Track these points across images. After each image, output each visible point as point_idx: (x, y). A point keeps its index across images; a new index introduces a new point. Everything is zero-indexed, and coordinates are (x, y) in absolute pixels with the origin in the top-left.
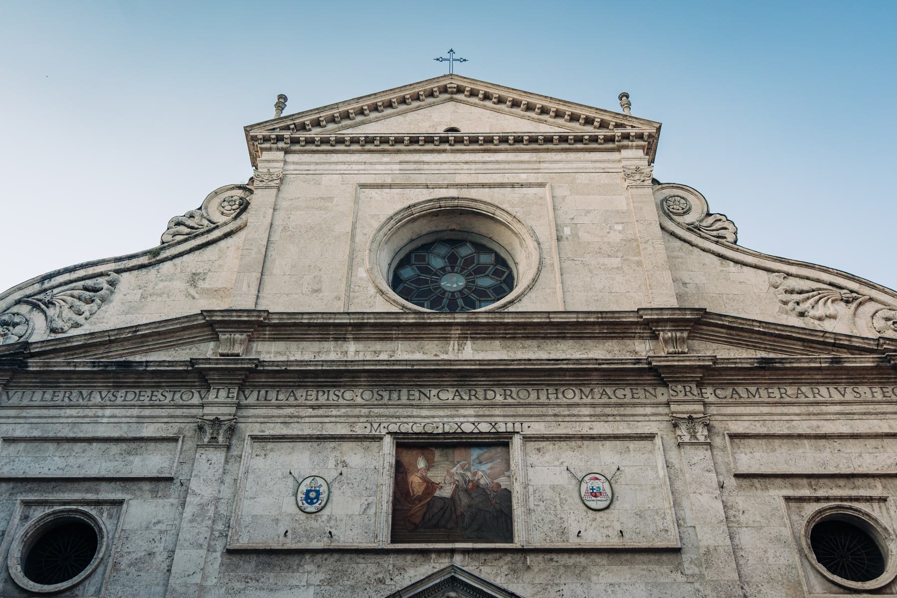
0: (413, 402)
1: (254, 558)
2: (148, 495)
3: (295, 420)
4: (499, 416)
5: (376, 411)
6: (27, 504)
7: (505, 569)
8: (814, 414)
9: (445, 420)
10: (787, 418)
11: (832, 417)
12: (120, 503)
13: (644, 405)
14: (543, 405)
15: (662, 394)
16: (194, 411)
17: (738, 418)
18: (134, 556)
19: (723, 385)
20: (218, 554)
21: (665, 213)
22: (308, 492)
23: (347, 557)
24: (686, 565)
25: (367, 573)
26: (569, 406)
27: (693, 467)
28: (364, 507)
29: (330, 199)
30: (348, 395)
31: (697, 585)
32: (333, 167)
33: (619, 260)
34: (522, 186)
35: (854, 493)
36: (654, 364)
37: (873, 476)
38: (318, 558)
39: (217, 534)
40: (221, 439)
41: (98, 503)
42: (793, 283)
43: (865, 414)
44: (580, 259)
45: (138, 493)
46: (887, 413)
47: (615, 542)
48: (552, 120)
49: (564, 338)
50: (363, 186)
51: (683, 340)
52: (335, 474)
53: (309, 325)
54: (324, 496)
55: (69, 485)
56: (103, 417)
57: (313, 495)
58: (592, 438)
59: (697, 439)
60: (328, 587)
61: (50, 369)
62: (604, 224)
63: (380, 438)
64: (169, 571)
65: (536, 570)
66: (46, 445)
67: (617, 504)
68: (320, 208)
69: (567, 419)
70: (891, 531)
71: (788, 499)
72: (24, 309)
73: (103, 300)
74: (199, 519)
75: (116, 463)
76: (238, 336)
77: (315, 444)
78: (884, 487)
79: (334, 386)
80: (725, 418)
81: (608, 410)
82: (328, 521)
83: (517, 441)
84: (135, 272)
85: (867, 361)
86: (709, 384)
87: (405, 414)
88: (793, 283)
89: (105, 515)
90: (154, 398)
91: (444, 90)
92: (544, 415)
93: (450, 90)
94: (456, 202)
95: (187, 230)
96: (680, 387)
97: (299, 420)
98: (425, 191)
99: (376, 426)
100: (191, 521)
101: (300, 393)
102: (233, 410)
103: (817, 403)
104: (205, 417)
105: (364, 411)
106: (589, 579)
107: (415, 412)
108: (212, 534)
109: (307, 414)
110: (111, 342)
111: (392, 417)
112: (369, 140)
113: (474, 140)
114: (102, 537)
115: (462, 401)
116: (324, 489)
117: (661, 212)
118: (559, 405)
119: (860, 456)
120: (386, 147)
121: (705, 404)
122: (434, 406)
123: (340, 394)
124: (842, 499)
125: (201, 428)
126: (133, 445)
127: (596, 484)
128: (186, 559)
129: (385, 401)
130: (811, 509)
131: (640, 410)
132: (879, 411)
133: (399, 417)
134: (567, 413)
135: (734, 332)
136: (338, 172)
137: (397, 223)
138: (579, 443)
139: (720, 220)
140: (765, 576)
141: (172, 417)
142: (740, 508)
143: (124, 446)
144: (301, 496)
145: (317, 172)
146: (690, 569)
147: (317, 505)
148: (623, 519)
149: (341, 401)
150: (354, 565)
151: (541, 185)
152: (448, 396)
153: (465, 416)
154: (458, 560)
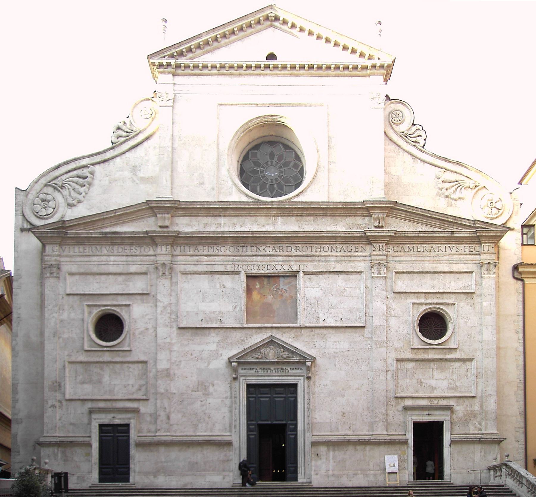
0: (254, 254)
1: (190, 331)
3: (199, 263)
5: (236, 258)
6: (89, 306)
7: (293, 335)
8: (436, 261)
9: (268, 263)
10: (423, 263)
12: (128, 306)
14: (313, 255)
15: (369, 249)
16: (152, 258)
17: (401, 262)
18: (141, 330)
19: (397, 245)
20: (175, 329)
23: (229, 330)
27: (376, 288)
28: (234, 307)
30: (223, 249)
31: (369, 342)
35: (442, 301)
36: (367, 234)
37: (453, 293)
38: (217, 330)
40: (167, 273)
46: (468, 261)
47: (339, 324)
51: (383, 219)
56: (110, 261)
58: (334, 273)
60: (222, 343)
64: (156, 336)
65: (306, 335)
66: (88, 276)
72: (50, 190)
73: (90, 184)
76: (166, 215)
77: (210, 276)
81: (343, 258)
83: (300, 275)
84: (102, 164)
85: (465, 233)
90: (132, 251)
93: (270, 18)
95: (125, 134)
96: (377, 245)
99: (237, 266)
100: (161, 314)
101: (200, 248)
102: (170, 258)
103: (438, 255)
104: (158, 262)
106: (327, 340)
107: (254, 259)
114: (125, 322)
115: (276, 253)
121: (387, 255)
122: (263, 256)
123: (219, 249)
124: (436, 304)
125: (157, 268)
126: (128, 277)
128: (162, 332)
129: (240, 253)
131: (358, 258)
132: (465, 259)
133: (247, 262)
134: (324, 260)
138: (328, 275)
140: (397, 338)
141: (142, 261)
146: (367, 334)
148: (343, 313)
149: (220, 253)
152: (270, 249)
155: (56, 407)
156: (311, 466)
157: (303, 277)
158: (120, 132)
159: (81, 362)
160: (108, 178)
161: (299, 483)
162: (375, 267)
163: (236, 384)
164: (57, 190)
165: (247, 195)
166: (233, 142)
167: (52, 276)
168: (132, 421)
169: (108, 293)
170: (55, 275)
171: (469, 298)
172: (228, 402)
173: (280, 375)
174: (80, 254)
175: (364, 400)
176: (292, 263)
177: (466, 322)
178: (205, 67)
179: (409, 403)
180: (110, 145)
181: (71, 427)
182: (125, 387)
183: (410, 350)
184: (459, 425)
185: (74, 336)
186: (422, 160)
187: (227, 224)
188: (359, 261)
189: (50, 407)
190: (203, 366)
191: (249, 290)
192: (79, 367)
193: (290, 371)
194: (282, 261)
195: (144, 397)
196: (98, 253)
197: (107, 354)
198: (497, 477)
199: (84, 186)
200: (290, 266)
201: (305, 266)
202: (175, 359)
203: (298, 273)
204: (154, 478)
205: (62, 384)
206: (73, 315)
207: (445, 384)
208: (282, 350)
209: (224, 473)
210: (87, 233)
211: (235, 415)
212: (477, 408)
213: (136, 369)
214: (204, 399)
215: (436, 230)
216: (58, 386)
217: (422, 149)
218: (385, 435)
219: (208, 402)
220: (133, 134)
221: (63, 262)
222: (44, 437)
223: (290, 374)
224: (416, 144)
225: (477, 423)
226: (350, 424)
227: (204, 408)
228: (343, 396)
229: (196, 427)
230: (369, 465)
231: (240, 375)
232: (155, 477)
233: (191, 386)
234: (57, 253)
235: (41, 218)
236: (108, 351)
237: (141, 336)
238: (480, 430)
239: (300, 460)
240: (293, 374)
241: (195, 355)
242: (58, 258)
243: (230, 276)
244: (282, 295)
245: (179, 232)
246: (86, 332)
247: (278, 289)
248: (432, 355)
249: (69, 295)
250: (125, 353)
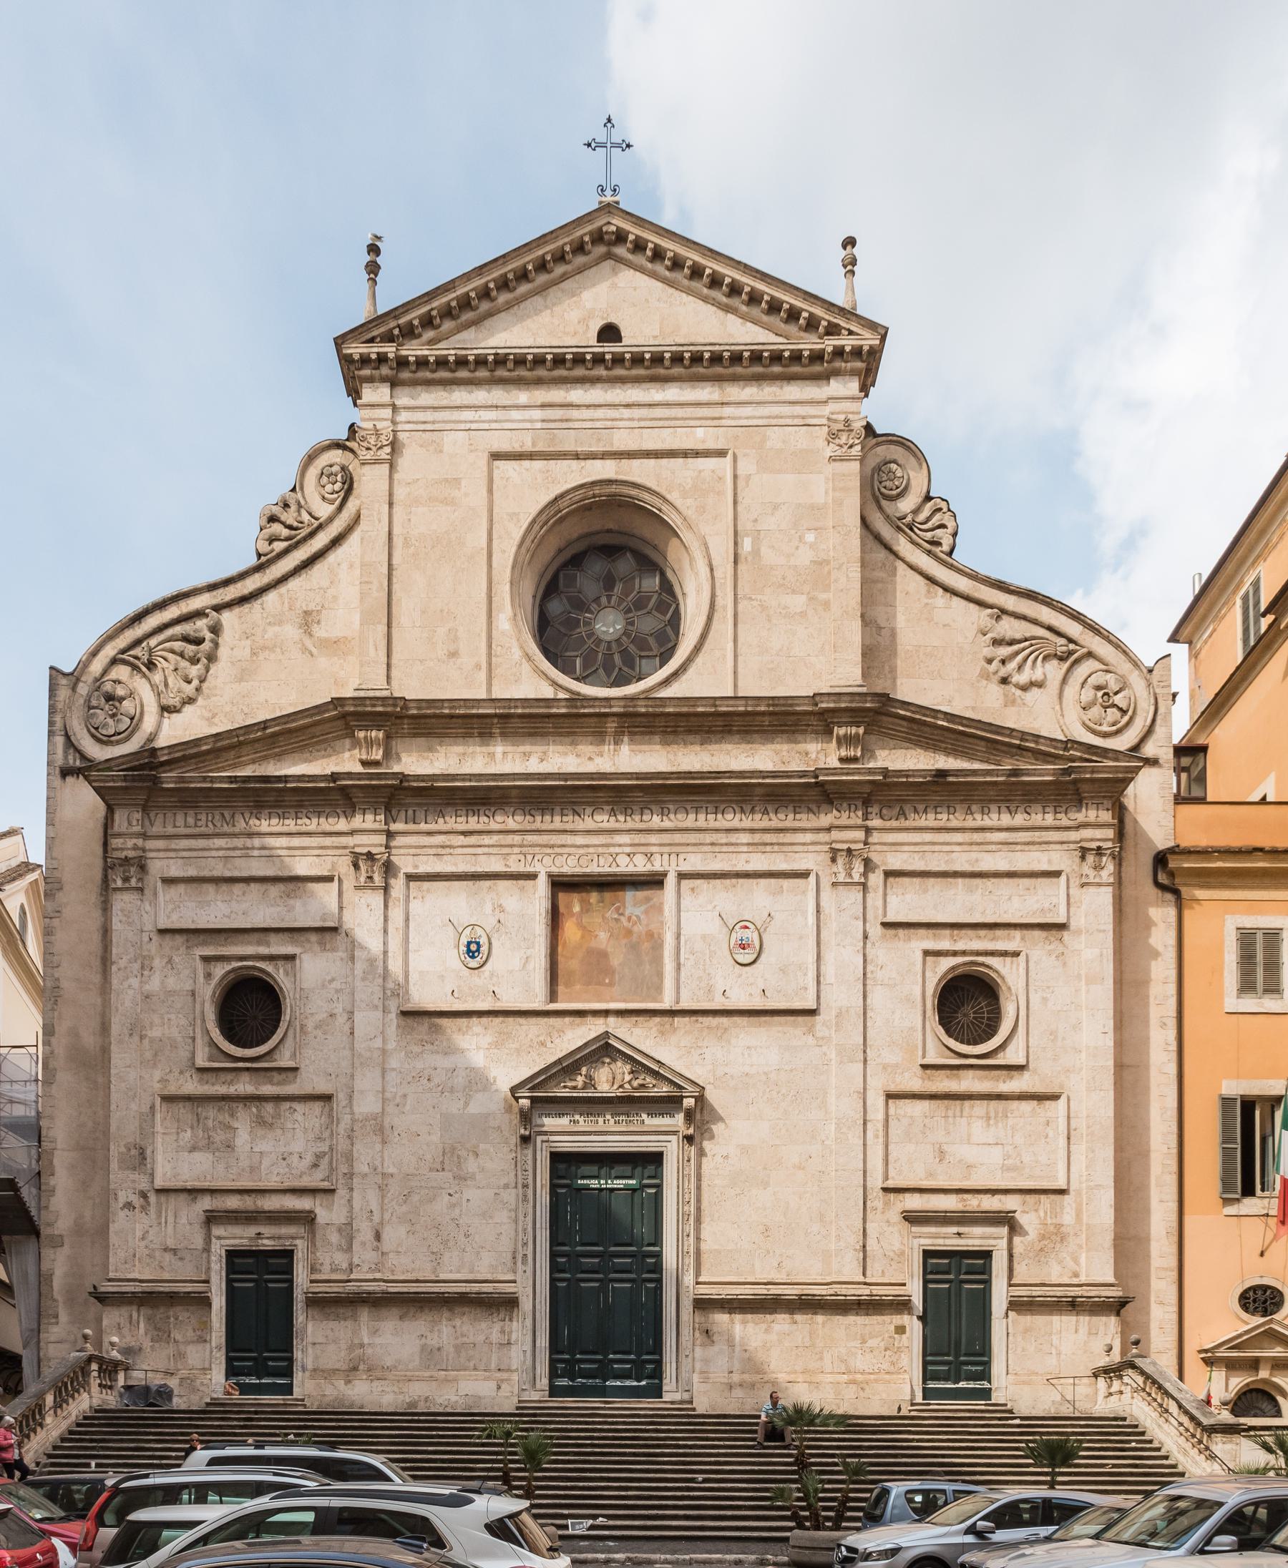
2: (317, 948)
3: (448, 851)
4: (654, 845)
6: (206, 959)
11: (993, 847)
13: (804, 830)
17: (898, 848)
20: (393, 1016)
21: (874, 495)
22: (469, 943)
24: (818, 1027)
25: (530, 1036)
26: (728, 830)
29: (457, 481)
32: (456, 415)
33: (804, 598)
34: (697, 454)
38: (484, 1020)
39: (389, 993)
41: (272, 958)
42: (1009, 628)
43: (1028, 843)
44: (759, 597)
45: (308, 946)
48: (744, 308)
49: (730, 732)
50: (496, 456)
52: (494, 922)
53: (451, 717)
54: (484, 949)
55: (240, 937)
56: (253, 848)
57: (473, 947)
59: (852, 878)
60: (496, 1051)
61: (186, 785)
62: (793, 532)
63: (532, 876)
64: (352, 1033)
67: (763, 956)
68: (446, 501)
69: (725, 849)
70: (1013, 991)
71: (927, 953)
74: (370, 977)
75: (279, 909)
77: (470, 883)
78: (1023, 939)
79: (484, 804)
80: (885, 848)
81: (768, 838)
82: (491, 979)
83: (671, 881)
85: (1044, 772)
86: (877, 801)
87: (559, 842)
88: (1009, 628)
89: (281, 971)
91: (598, 237)
92: (701, 844)
93: (606, 237)
94: (613, 489)
97: (452, 851)
98: (574, 464)
99: (529, 857)
100: (363, 979)
104: (358, 850)
105: (517, 839)
107: (569, 839)
108: (384, 993)
109: (459, 844)
110: (240, 744)
111: (546, 846)
112: (500, 361)
113: (638, 360)
114: (285, 999)
116: (483, 941)
117: (869, 494)
118: (717, 830)
119: (1010, 899)
120: (522, 372)
124: (978, 953)
127: (747, 933)
128: (367, 1021)
130: (947, 963)
131: (800, 837)
133: (552, 846)
134: (724, 841)
135: (915, 727)
136: (462, 426)
137: (541, 528)
138: (734, 881)
139: (940, 509)
140: (888, 1039)
141: (322, 848)
142: (880, 963)
143: (281, 887)
144: (463, 949)
145: (437, 426)
147: (478, 959)
150: (518, 1027)
151: (721, 453)
152: (603, 820)
153: (620, 845)
154: (612, 1024)
155: (134, 1208)
157: (679, 884)
158: (277, 528)
159: (188, 1098)
160: (248, 642)
162: (840, 861)
163: (529, 1152)
164: (139, 670)
165: (554, 683)
166: (523, 550)
167: (127, 885)
168: (298, 1242)
169: (249, 926)
170: (133, 882)
171: (1052, 939)
172: (510, 1196)
174: (188, 831)
175: (812, 1195)
176: (654, 849)
177: (1045, 1000)
178: (462, 362)
179: (915, 1202)
180: (252, 561)
181: (168, 1256)
182: (284, 1159)
183: (919, 1071)
184: (1026, 1261)
185: (175, 1032)
186: (946, 589)
187: (510, 756)
188: (804, 844)
189: (122, 1209)
190: (453, 1106)
191: (555, 918)
192: (183, 1110)
193: (646, 1122)
194: (631, 845)
195: (326, 1185)
196: (226, 829)
197: (245, 1077)
198: (1111, 1394)
199: (198, 661)
200: (649, 856)
201: (681, 857)
202: (394, 1090)
203: (666, 875)
204: (346, 1384)
205: (148, 1152)
206: (171, 983)
207: (996, 1155)
209: (499, 1375)
210: (204, 779)
211: (525, 1230)
212: (1068, 1218)
213: (306, 1118)
214: (457, 1188)
215: (977, 766)
216: (140, 1158)
217: (948, 559)
218: (859, 1283)
219: (465, 1196)
220: (303, 533)
221: (151, 850)
222: (110, 1280)
224: (933, 548)
225: (1068, 1258)
226: (781, 1255)
227: (457, 1211)
228: (765, 1185)
229: (437, 1257)
230: (821, 1359)
232: (348, 1382)
233: (428, 1157)
234: (137, 829)
235: (104, 741)
236: (248, 1069)
237: (319, 1033)
238: (1076, 1275)
241: (436, 1080)
242: (140, 842)
243: (514, 882)
244: (629, 932)
245: (403, 777)
246: (199, 1022)
247: (622, 914)
248: (969, 1082)
249: (163, 932)
250: (283, 1076)
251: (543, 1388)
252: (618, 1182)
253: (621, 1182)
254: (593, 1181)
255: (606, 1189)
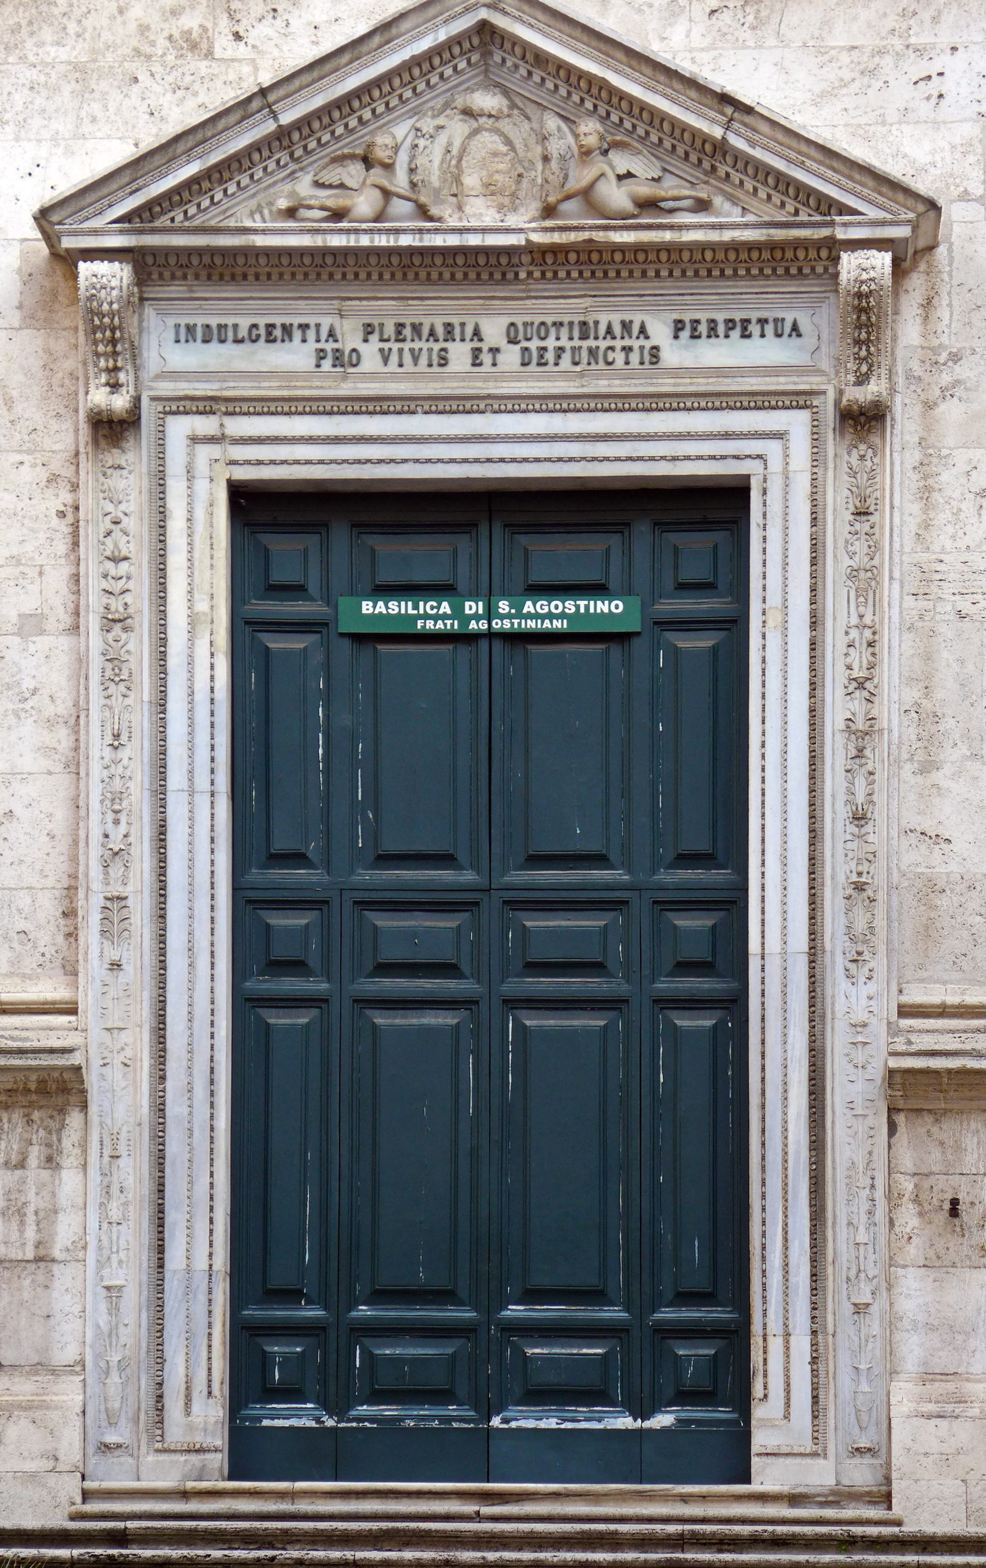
156: (892, 1322)
161: (763, 1498)
173: (571, 387)
193: (673, 355)
208: (590, 129)
223: (666, 385)
231: (167, 388)
239: (775, 1258)
240: (702, 385)
251: (198, 1439)
252: (542, 606)
253: (556, 606)
254: (427, 606)
255: (491, 635)
